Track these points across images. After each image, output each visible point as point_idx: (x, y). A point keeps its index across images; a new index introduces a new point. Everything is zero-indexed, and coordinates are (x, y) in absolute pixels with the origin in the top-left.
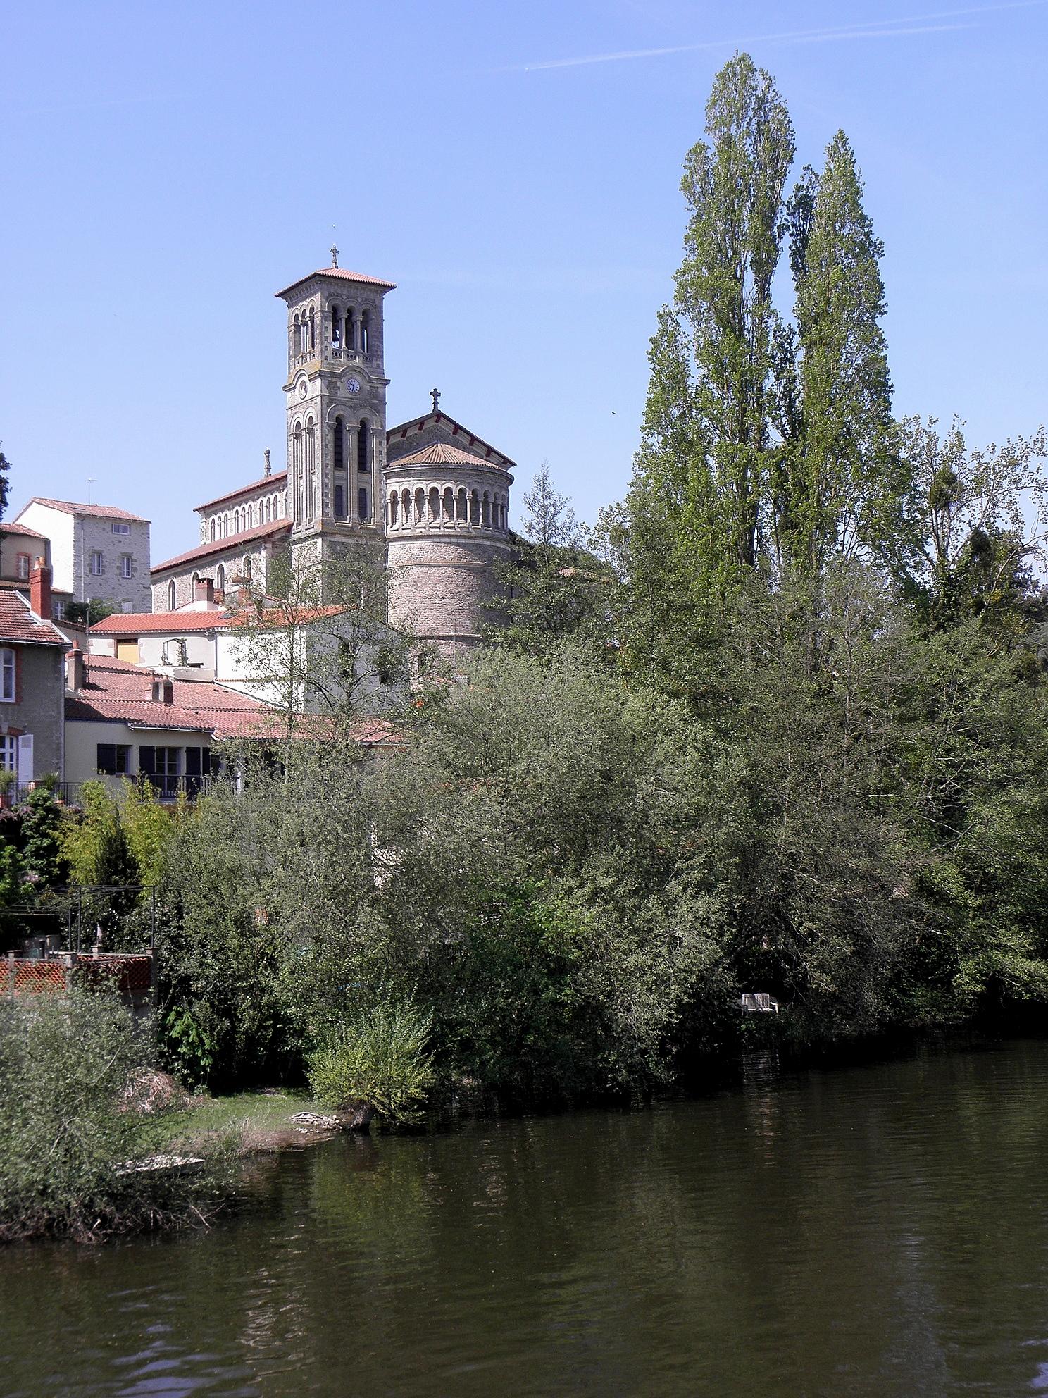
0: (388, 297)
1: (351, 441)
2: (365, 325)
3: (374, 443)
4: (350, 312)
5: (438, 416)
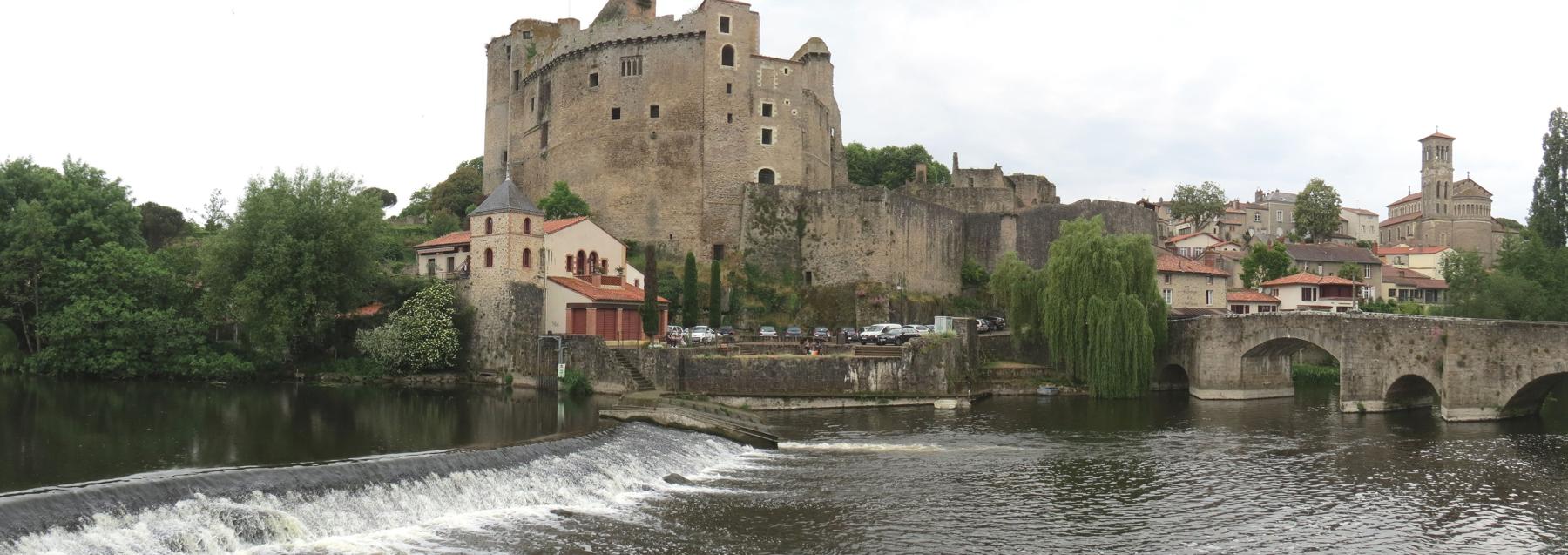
0: (1454, 141)
2: (1447, 151)
4: (1443, 147)
5: (1469, 180)
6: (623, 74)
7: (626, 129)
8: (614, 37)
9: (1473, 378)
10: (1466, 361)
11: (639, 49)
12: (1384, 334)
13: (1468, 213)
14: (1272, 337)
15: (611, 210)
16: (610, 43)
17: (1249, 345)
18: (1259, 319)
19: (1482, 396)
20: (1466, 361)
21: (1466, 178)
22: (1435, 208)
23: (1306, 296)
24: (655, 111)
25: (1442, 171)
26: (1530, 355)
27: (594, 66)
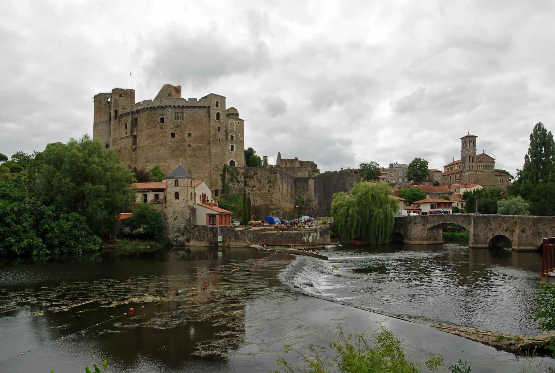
0: (477, 138)
1: (471, 159)
4: (471, 141)
5: (484, 154)
7: (177, 142)
8: (172, 104)
9: (527, 236)
10: (525, 230)
11: (182, 110)
12: (488, 221)
13: (484, 168)
14: (441, 223)
16: (170, 106)
17: (429, 226)
18: (435, 217)
19: (530, 242)
20: (525, 230)
22: (468, 167)
23: (432, 207)
24: (190, 135)
25: (471, 151)
26: (551, 228)
27: (162, 115)
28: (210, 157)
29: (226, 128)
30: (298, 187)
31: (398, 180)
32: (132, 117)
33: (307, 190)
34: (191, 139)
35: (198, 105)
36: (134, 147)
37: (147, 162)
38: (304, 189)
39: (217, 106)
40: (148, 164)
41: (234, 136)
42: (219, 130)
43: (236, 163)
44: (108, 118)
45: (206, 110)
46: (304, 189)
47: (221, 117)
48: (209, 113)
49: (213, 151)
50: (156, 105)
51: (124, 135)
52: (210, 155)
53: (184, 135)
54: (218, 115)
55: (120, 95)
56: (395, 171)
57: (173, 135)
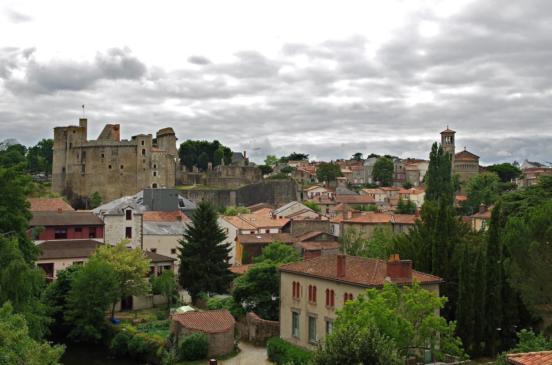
0: (455, 134)
3: (452, 157)
5: (465, 151)
6: (112, 155)
7: (113, 172)
8: (110, 144)
13: (461, 168)
15: (108, 195)
21: (464, 150)
24: (122, 167)
27: (102, 152)
28: (136, 183)
29: (150, 160)
30: (221, 198)
31: (367, 180)
32: (82, 150)
33: (229, 201)
34: (123, 170)
35: (128, 145)
36: (83, 173)
37: (92, 186)
38: (226, 200)
39: (143, 144)
40: (92, 187)
41: (157, 164)
42: (144, 162)
43: (158, 185)
44: (64, 147)
45: (134, 148)
46: (226, 200)
47: (146, 152)
48: (136, 150)
49: (138, 178)
50: (99, 144)
51: (76, 163)
52: (136, 181)
53: (118, 166)
54: (144, 151)
55: (74, 132)
56: (364, 170)
57: (110, 167)
